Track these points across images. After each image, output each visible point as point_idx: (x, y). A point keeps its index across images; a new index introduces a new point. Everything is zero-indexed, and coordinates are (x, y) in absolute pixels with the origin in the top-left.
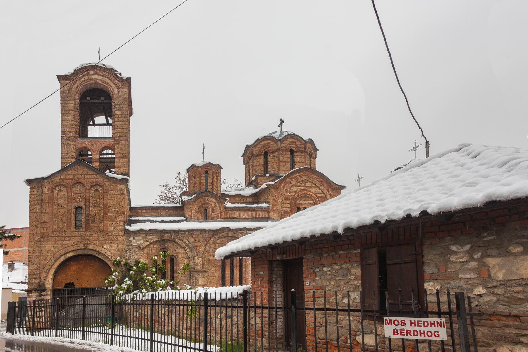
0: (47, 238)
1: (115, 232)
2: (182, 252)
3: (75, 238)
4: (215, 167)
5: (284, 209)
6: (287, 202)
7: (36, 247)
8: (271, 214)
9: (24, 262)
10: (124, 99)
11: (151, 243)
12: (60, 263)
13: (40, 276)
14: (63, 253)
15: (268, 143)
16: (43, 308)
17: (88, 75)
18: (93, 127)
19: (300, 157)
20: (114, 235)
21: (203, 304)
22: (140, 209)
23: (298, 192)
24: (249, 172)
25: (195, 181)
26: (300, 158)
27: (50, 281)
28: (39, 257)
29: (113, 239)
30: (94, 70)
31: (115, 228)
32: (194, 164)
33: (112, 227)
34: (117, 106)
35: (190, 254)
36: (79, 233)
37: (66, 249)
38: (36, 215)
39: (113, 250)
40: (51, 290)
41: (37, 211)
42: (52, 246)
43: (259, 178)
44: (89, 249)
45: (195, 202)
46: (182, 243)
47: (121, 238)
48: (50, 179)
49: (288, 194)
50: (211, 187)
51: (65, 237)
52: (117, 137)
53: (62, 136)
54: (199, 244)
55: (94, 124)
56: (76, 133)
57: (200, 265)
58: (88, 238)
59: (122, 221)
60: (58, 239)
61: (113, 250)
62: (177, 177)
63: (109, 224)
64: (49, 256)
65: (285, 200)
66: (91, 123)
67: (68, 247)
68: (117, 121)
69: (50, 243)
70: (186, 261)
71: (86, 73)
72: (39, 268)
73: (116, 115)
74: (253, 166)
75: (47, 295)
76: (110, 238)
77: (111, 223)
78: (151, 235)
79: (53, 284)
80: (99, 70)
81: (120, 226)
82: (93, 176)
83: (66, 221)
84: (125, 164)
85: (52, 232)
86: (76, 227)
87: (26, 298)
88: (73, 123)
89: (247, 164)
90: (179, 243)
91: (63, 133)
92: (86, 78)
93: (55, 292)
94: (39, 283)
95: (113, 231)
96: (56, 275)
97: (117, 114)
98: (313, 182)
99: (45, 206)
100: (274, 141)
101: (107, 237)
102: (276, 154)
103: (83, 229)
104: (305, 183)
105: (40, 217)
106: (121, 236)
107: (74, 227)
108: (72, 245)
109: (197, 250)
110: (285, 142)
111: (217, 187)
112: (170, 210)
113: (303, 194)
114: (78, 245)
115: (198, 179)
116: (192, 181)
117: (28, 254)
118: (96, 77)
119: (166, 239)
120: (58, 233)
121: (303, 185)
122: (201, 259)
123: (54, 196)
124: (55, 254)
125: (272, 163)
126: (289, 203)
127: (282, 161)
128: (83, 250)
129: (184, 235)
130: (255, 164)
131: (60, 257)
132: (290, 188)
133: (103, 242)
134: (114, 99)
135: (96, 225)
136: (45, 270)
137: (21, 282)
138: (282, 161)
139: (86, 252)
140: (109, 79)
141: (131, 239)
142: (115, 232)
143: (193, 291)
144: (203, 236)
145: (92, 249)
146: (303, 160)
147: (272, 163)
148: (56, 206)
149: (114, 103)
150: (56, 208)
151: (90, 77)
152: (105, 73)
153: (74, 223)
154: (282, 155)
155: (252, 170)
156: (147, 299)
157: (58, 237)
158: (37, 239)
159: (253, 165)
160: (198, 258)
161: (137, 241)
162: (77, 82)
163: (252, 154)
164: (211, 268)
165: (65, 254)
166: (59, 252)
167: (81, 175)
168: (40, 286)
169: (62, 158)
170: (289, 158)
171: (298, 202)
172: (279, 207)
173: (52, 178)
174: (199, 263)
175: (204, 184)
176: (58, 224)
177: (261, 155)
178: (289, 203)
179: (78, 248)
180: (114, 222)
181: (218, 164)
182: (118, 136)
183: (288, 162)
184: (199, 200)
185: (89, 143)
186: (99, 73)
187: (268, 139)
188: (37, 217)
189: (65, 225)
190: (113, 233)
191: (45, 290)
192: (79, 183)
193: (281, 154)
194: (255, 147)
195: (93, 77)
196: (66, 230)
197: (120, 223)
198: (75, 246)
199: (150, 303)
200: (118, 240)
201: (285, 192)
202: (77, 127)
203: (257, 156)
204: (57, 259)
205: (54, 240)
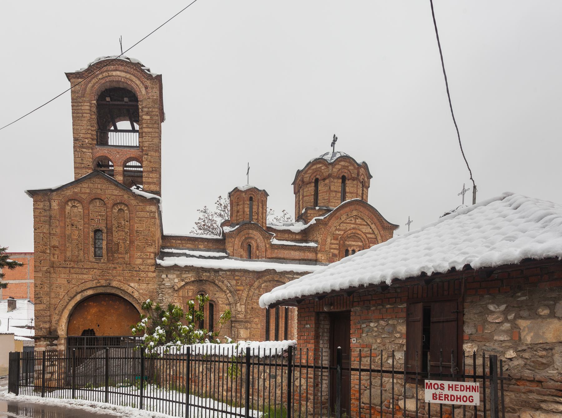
0: (58, 269)
1: (144, 267)
2: (223, 297)
3: (94, 271)
4: (260, 193)
5: (332, 251)
6: (335, 242)
7: (44, 279)
8: (319, 255)
9: (29, 300)
10: (154, 101)
11: (187, 284)
12: (76, 302)
13: (50, 319)
14: (80, 290)
15: (320, 168)
16: (56, 361)
17: (106, 71)
18: (115, 133)
19: (352, 185)
20: (143, 270)
21: (245, 361)
22: (174, 238)
23: (348, 231)
24: (299, 203)
25: (238, 208)
26: (352, 187)
27: (63, 326)
28: (48, 294)
29: (142, 275)
30: (115, 65)
31: (144, 261)
32: (237, 188)
33: (141, 260)
34: (145, 110)
35: (231, 300)
36: (100, 264)
37: (83, 285)
38: (43, 236)
39: (141, 289)
40: (65, 338)
41: (45, 231)
42: (66, 280)
43: (309, 212)
44: (112, 287)
45: (237, 235)
48: (60, 191)
49: (337, 232)
50: (256, 217)
51: (82, 268)
52: (145, 147)
53: (74, 143)
55: (116, 130)
56: (93, 139)
57: (243, 314)
58: (111, 271)
59: (152, 253)
60: (72, 271)
61: (141, 289)
62: (218, 201)
63: (136, 256)
64: (62, 293)
65: (334, 239)
66: (112, 128)
67: (85, 282)
68: (144, 128)
69: (63, 276)
70: (227, 308)
71: (105, 69)
72: (49, 308)
73: (144, 121)
74: (303, 196)
75: (60, 344)
77: (139, 254)
78: (187, 272)
79: (67, 330)
80: (122, 65)
81: (150, 259)
82: (116, 192)
83: (83, 248)
84: (155, 180)
85: (65, 261)
86: (95, 256)
87: (33, 347)
88: (88, 128)
89: (297, 193)
91: (76, 140)
92: (104, 74)
93: (70, 341)
94: (50, 328)
95: (142, 265)
96: (71, 318)
97: (145, 119)
98: (365, 218)
99: (55, 225)
100: (325, 165)
101: (135, 273)
102: (327, 181)
103: (104, 260)
104: (356, 219)
105: (48, 240)
106: (152, 272)
107: (93, 256)
108: (91, 281)
109: (239, 296)
110: (337, 166)
111: (263, 219)
112: (209, 243)
113: (352, 233)
115: (241, 207)
116: (235, 208)
117: (34, 289)
118: (118, 73)
119: (204, 279)
120: (72, 263)
121: (353, 222)
122: (243, 306)
123: (67, 213)
124: (68, 291)
125: (323, 192)
126: (337, 244)
127: (332, 191)
128: (105, 288)
129: (225, 276)
130: (305, 194)
131: (75, 296)
132: (339, 225)
134: (141, 101)
135: (120, 256)
136: (57, 312)
137: (26, 326)
138: (332, 191)
139: (109, 291)
140: (134, 75)
141: (164, 276)
143: (235, 345)
144: (246, 278)
145: (116, 286)
146: (355, 190)
147: (323, 192)
148: (70, 226)
149: (141, 105)
150: (70, 229)
151: (110, 73)
152: (129, 69)
153: (93, 251)
154: (333, 183)
155: (302, 201)
156: (182, 353)
157: (73, 268)
158: (45, 269)
159: (303, 195)
160: (241, 305)
161: (170, 280)
162: (93, 80)
163: (303, 182)
164: (254, 318)
165: (82, 291)
166: (75, 288)
167: (101, 189)
168: (51, 333)
169: (75, 168)
170: (340, 187)
171: (347, 243)
172: (327, 248)
173: (63, 191)
174: (241, 311)
175: (248, 213)
176: (72, 251)
177: (312, 182)
178: (337, 244)
179: (98, 285)
180: (143, 253)
181: (264, 190)
182: (147, 145)
183: (338, 192)
184: (242, 233)
185: (110, 151)
186: (122, 68)
187: (319, 163)
188: (45, 240)
189: (81, 253)
190: (142, 267)
191: (57, 338)
192: (98, 199)
193: (332, 182)
194: (306, 173)
195: (114, 73)
196: (83, 260)
197: (150, 255)
198: (94, 282)
199: (186, 358)
200: (147, 276)
201: (334, 229)
202: (94, 133)
203: (307, 184)
204: (72, 298)
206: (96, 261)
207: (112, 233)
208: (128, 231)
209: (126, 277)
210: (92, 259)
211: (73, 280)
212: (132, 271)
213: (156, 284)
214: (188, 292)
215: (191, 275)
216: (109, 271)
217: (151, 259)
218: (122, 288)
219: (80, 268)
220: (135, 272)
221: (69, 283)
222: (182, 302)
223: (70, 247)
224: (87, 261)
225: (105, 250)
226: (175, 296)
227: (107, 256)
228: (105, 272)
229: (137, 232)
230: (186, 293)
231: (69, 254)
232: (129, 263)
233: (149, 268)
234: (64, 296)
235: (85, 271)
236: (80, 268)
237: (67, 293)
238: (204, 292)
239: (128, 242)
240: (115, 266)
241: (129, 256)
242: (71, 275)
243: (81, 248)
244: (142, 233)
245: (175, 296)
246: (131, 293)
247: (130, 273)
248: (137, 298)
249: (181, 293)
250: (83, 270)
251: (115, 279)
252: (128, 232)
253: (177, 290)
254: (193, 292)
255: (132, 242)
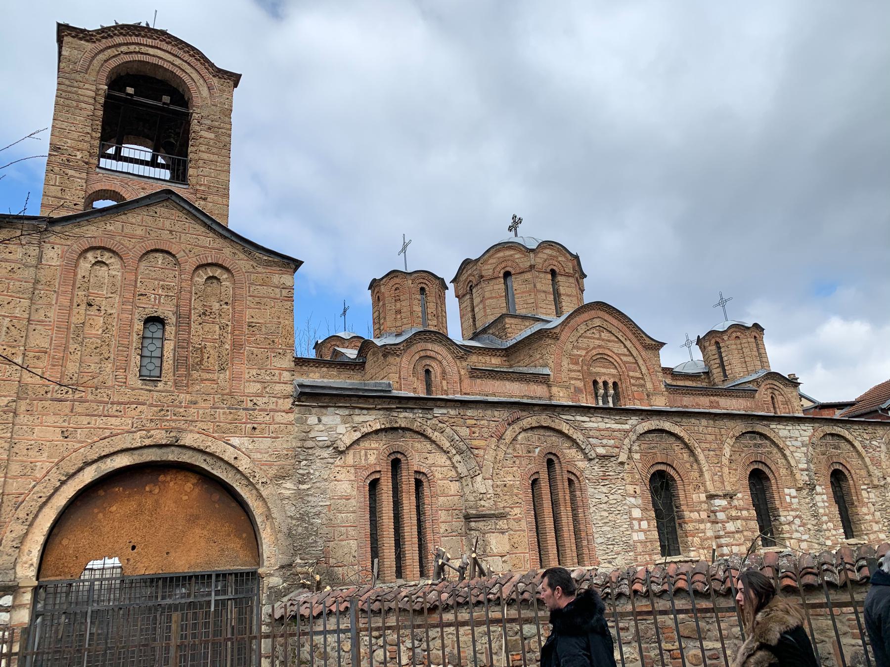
1: (265, 400)
2: (443, 464)
3: (139, 410)
11: (365, 436)
14: (95, 457)
20: (263, 406)
29: (260, 419)
31: (265, 388)
33: (259, 386)
42: (58, 430)
46: (443, 438)
47: (280, 417)
54: (482, 443)
58: (182, 410)
60: (79, 408)
64: (43, 463)
69: (51, 419)
76: (251, 415)
90: (434, 438)
101: (242, 413)
108: (128, 432)
114: (148, 431)
119: (403, 426)
131: (80, 469)
133: (229, 426)
135: (205, 376)
141: (312, 420)
142: (265, 400)
145: (195, 445)
157: (82, 401)
165: (101, 458)
166: (82, 450)
179: (147, 442)
180: (263, 371)
189: (108, 367)
190: (260, 401)
197: (280, 374)
200: (273, 422)
205: (67, 411)
206: (144, 387)
207: (189, 324)
208: (229, 323)
209: (222, 424)
210: (134, 381)
211: (79, 431)
212: (236, 409)
213: (295, 438)
214: (366, 455)
215: (374, 417)
216: (177, 409)
217: (283, 383)
218: (208, 450)
219: (101, 402)
220: (245, 412)
221: (66, 438)
222: (353, 478)
223: (79, 353)
224: (122, 386)
225: (171, 362)
226: (338, 466)
227: (174, 376)
228: (168, 411)
229: (250, 326)
230: (363, 458)
231: (72, 367)
232: (227, 391)
233: (277, 402)
234: (48, 473)
235: (114, 409)
236: (101, 402)
237: (57, 464)
238: (402, 454)
239: (227, 346)
240: (194, 399)
241: (227, 377)
242: (73, 419)
243: (106, 356)
244: (263, 329)
245: (338, 466)
246: (232, 462)
247: (231, 413)
248: (246, 472)
249: (350, 458)
250: (110, 406)
251: (191, 428)
252: (227, 325)
253: (342, 452)
254: (378, 454)
255: (237, 346)
